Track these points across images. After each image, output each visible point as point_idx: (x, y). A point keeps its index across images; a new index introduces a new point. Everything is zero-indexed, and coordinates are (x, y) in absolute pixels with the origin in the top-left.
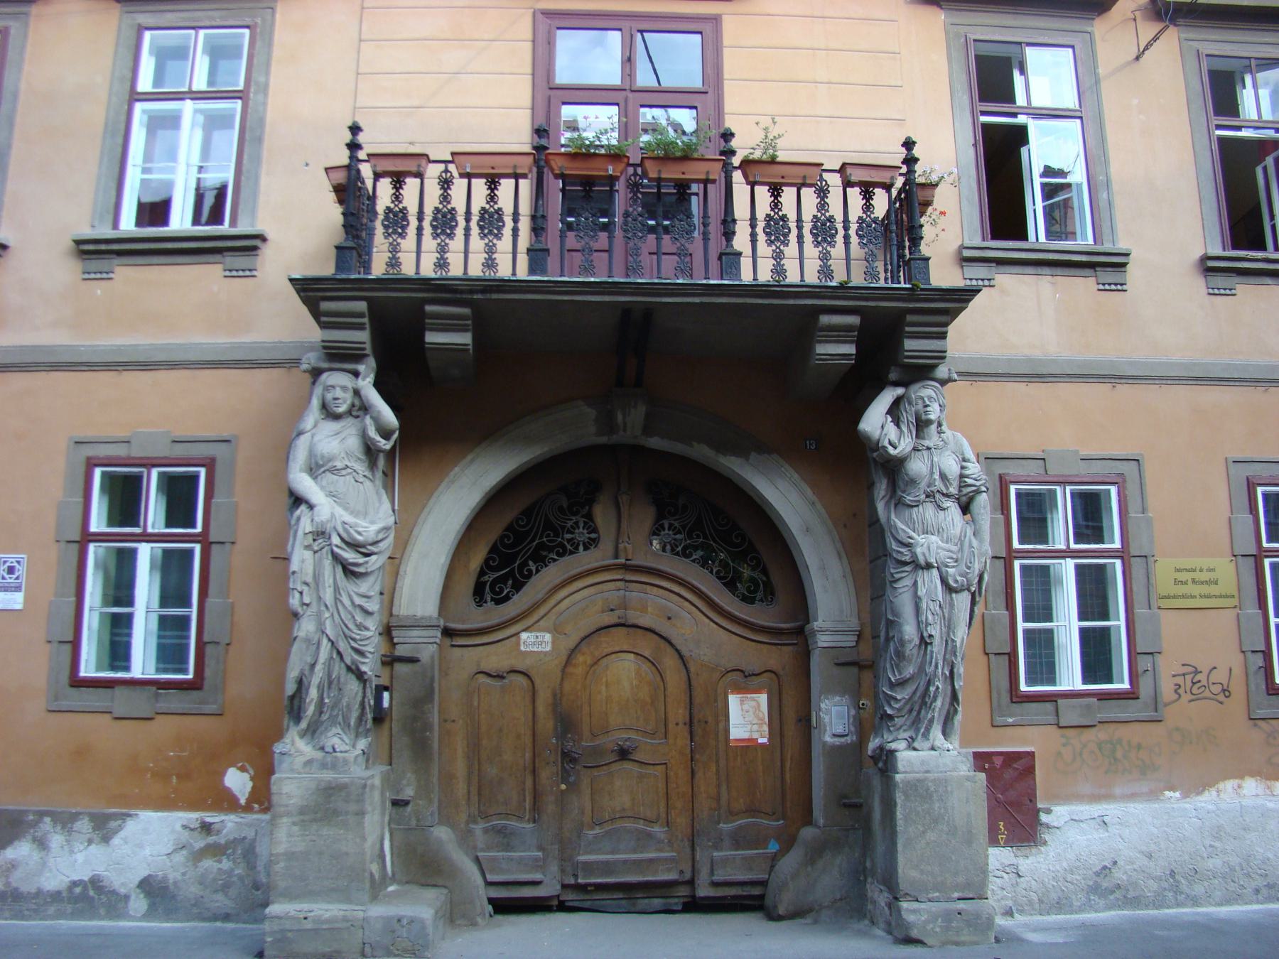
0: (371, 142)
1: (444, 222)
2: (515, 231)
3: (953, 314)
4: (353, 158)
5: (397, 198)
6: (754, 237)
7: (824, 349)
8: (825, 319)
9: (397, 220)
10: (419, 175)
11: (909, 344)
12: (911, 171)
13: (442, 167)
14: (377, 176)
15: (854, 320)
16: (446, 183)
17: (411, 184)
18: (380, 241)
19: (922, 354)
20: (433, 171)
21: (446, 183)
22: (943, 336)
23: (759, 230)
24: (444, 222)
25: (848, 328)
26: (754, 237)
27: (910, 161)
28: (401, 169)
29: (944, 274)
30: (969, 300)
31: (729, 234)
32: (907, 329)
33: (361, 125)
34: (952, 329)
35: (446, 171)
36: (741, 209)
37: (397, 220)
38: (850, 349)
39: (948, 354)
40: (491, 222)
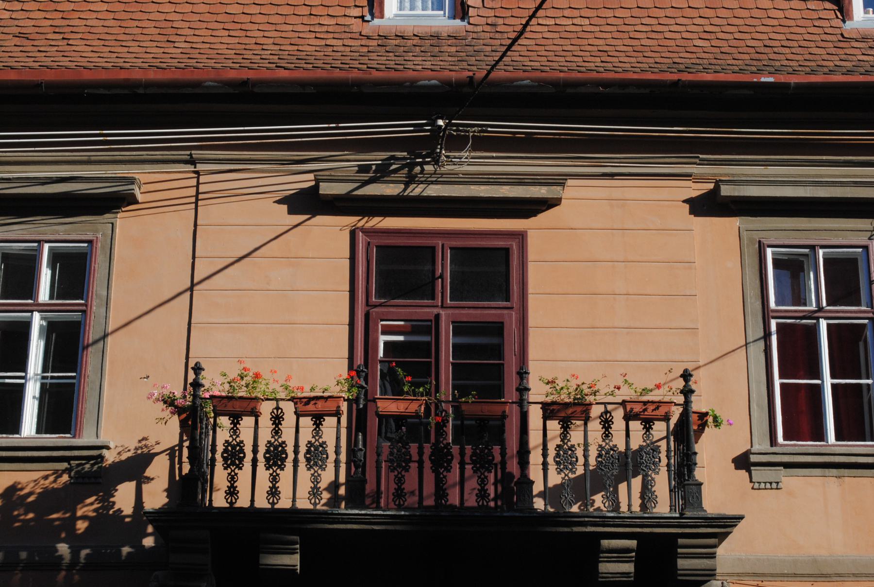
0: (215, 384)
1: (276, 457)
2: (337, 462)
3: (722, 537)
4: (195, 396)
5: (235, 432)
6: (545, 465)
7: (607, 568)
8: (605, 543)
9: (234, 456)
10: (256, 414)
11: (682, 563)
12: (687, 404)
13: (273, 404)
14: (217, 414)
15: (633, 543)
16: (277, 419)
17: (247, 422)
18: (221, 476)
19: (694, 572)
20: (266, 409)
21: (277, 419)
22: (712, 556)
23: (550, 460)
24: (276, 457)
25: (627, 550)
26: (545, 465)
27: (687, 392)
28: (238, 407)
29: (714, 501)
30: (736, 526)
31: (524, 463)
32: (679, 550)
33: (203, 366)
34: (720, 551)
35: (278, 408)
36: (535, 438)
37: (234, 456)
38: (629, 568)
39: (718, 571)
40: (315, 455)
